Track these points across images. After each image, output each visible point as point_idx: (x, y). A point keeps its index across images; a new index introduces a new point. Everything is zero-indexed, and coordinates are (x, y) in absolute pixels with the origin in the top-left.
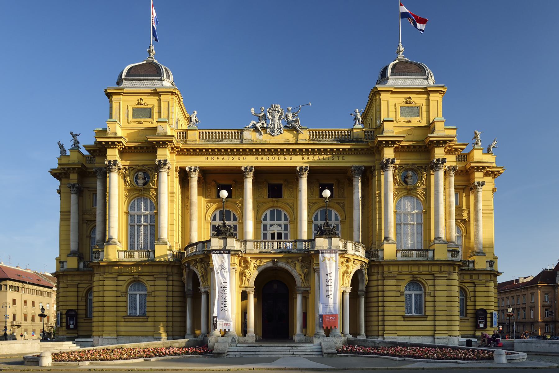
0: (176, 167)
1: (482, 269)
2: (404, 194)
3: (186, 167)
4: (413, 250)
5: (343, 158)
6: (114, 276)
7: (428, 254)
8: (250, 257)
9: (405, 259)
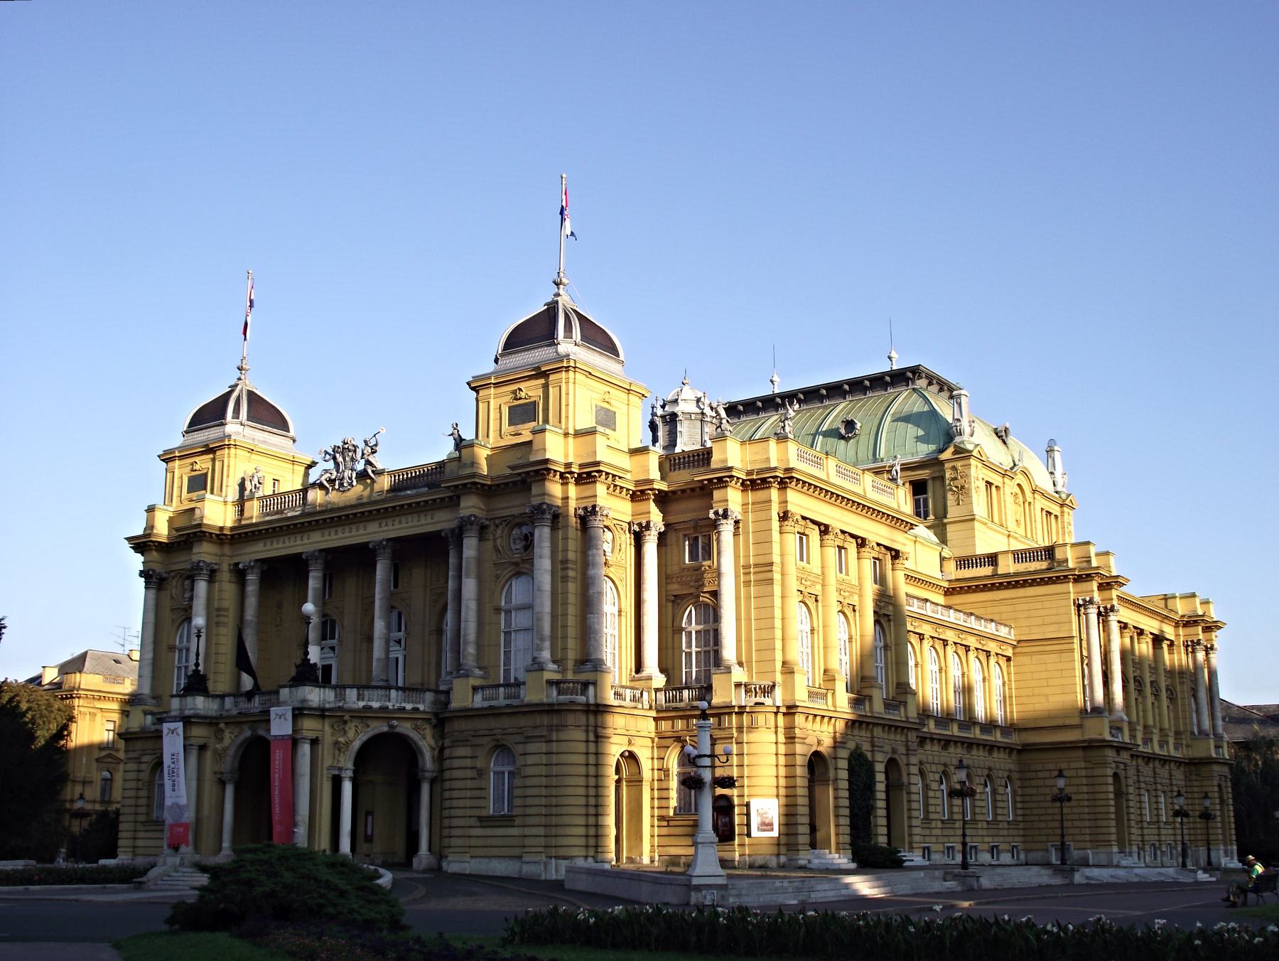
0: (230, 565)
1: (723, 705)
2: (511, 573)
4: (499, 686)
6: (136, 756)
7: (519, 693)
9: (486, 704)
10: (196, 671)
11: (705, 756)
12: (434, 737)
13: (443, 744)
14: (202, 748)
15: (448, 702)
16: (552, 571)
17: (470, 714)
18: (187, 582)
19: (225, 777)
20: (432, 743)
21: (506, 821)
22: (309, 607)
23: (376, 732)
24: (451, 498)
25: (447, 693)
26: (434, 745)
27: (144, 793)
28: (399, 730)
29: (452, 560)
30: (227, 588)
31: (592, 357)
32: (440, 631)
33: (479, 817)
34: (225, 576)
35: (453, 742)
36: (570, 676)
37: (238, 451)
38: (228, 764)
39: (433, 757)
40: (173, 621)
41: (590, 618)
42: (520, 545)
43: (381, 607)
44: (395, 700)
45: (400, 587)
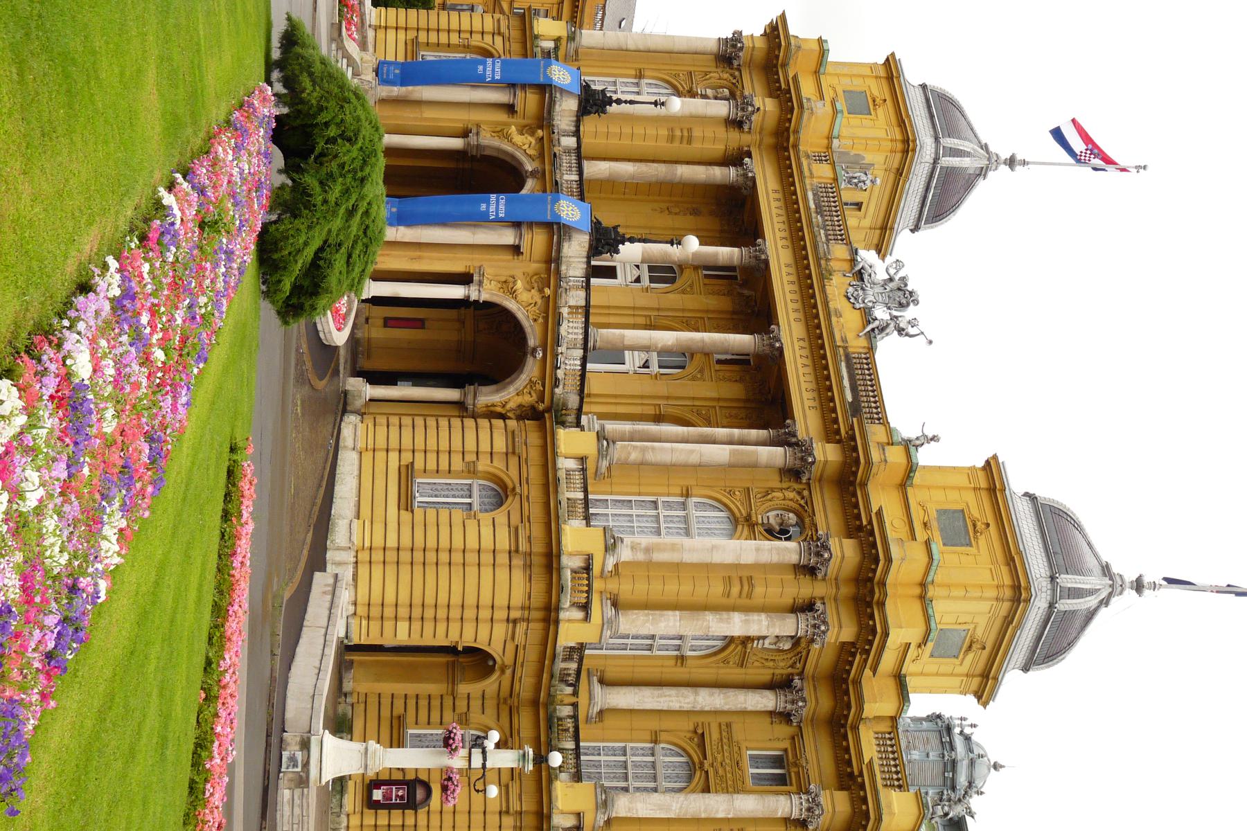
0: (749, 146)
3: (750, 156)
4: (586, 491)
5: (813, 407)
8: (543, 138)
9: (562, 474)
10: (610, 102)
11: (485, 759)
12: (520, 406)
13: (510, 418)
14: (510, 108)
15: (563, 424)
16: (740, 564)
17: (548, 452)
18: (726, 92)
19: (473, 139)
20: (511, 405)
21: (406, 502)
22: (692, 244)
23: (528, 330)
24: (838, 432)
25: (578, 424)
26: (508, 407)
27: (454, 39)
28: (530, 360)
29: (754, 433)
30: (722, 141)
31: (1034, 626)
32: (658, 419)
33: (412, 463)
34: (735, 139)
35: (513, 432)
36: (597, 585)
37: (899, 155)
38: (488, 139)
39: (493, 405)
40: (676, 76)
41: (674, 616)
42: (773, 518)
43: (692, 340)
44: (570, 360)
45: (718, 367)
